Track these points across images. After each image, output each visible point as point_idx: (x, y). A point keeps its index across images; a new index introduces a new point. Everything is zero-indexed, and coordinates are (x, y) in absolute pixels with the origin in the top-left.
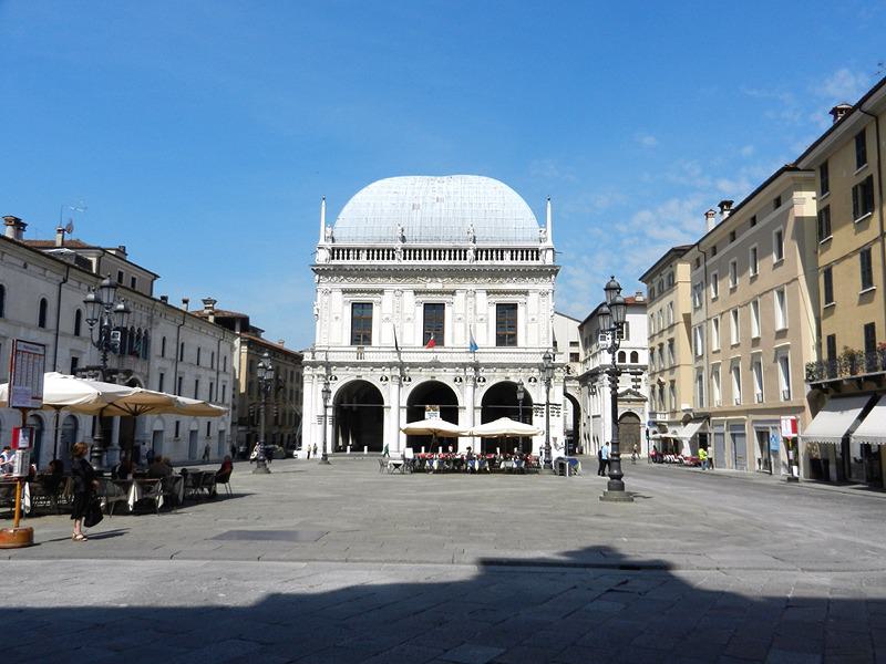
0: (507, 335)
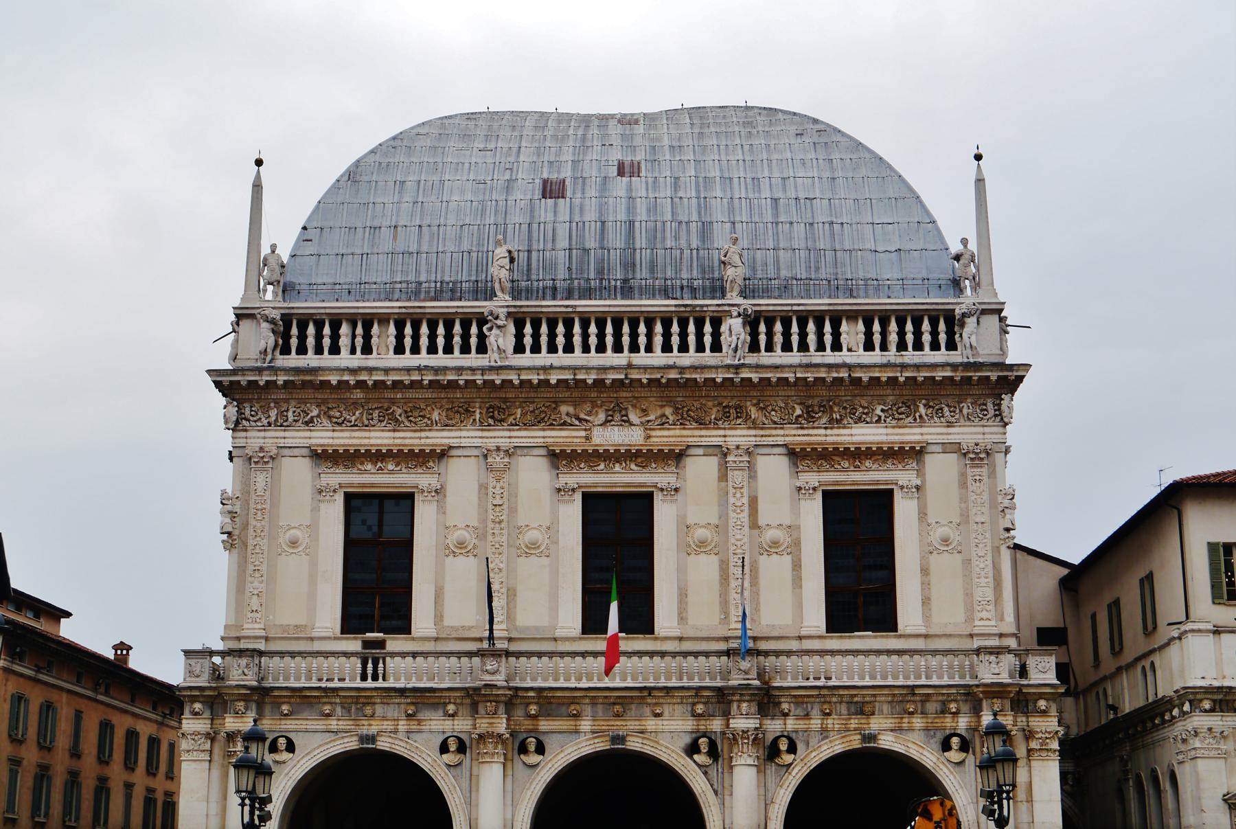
0: (861, 588)
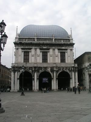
0: (63, 60)
